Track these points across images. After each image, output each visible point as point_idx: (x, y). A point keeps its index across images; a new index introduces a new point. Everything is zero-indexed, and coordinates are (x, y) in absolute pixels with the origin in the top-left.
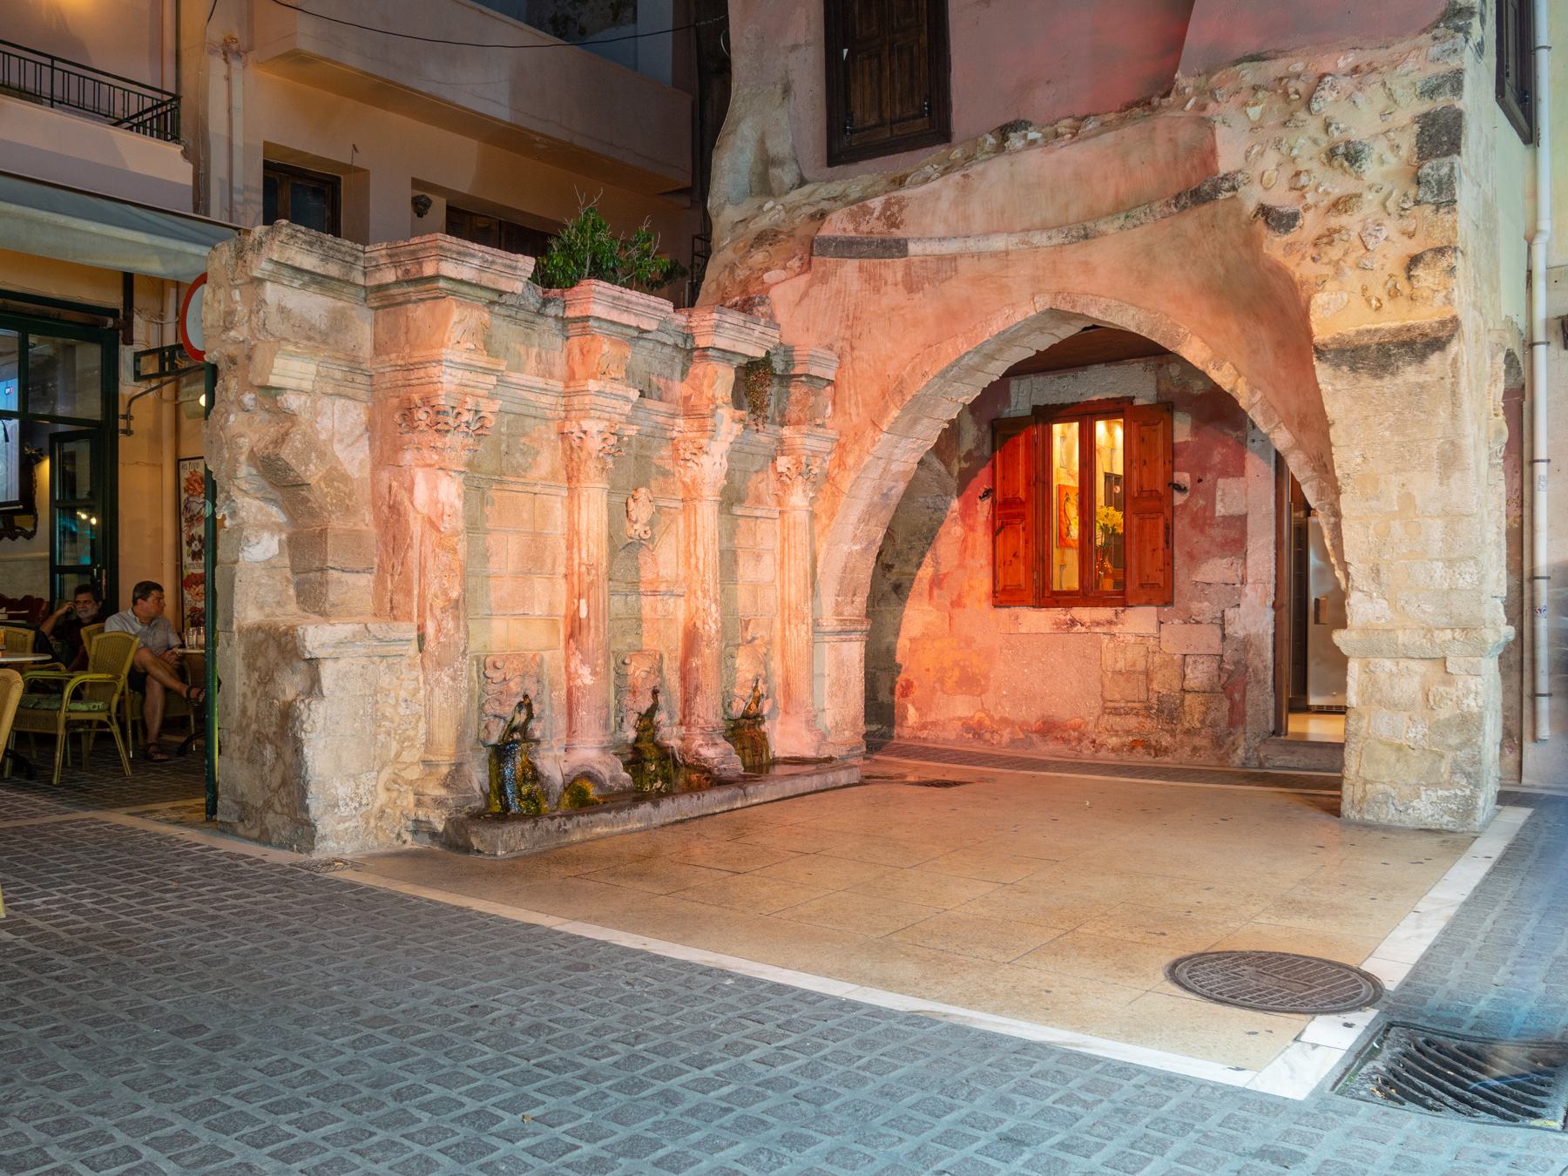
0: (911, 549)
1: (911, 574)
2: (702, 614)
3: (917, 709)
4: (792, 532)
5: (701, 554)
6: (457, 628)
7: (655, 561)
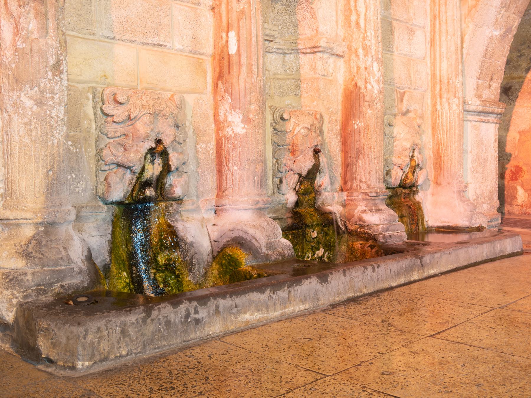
0: (521, 56)
1: (520, 78)
2: (363, 72)
3: (525, 190)
4: (443, 9)
5: (362, 10)
6: (44, 30)
7: (314, 16)
